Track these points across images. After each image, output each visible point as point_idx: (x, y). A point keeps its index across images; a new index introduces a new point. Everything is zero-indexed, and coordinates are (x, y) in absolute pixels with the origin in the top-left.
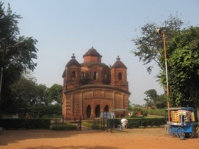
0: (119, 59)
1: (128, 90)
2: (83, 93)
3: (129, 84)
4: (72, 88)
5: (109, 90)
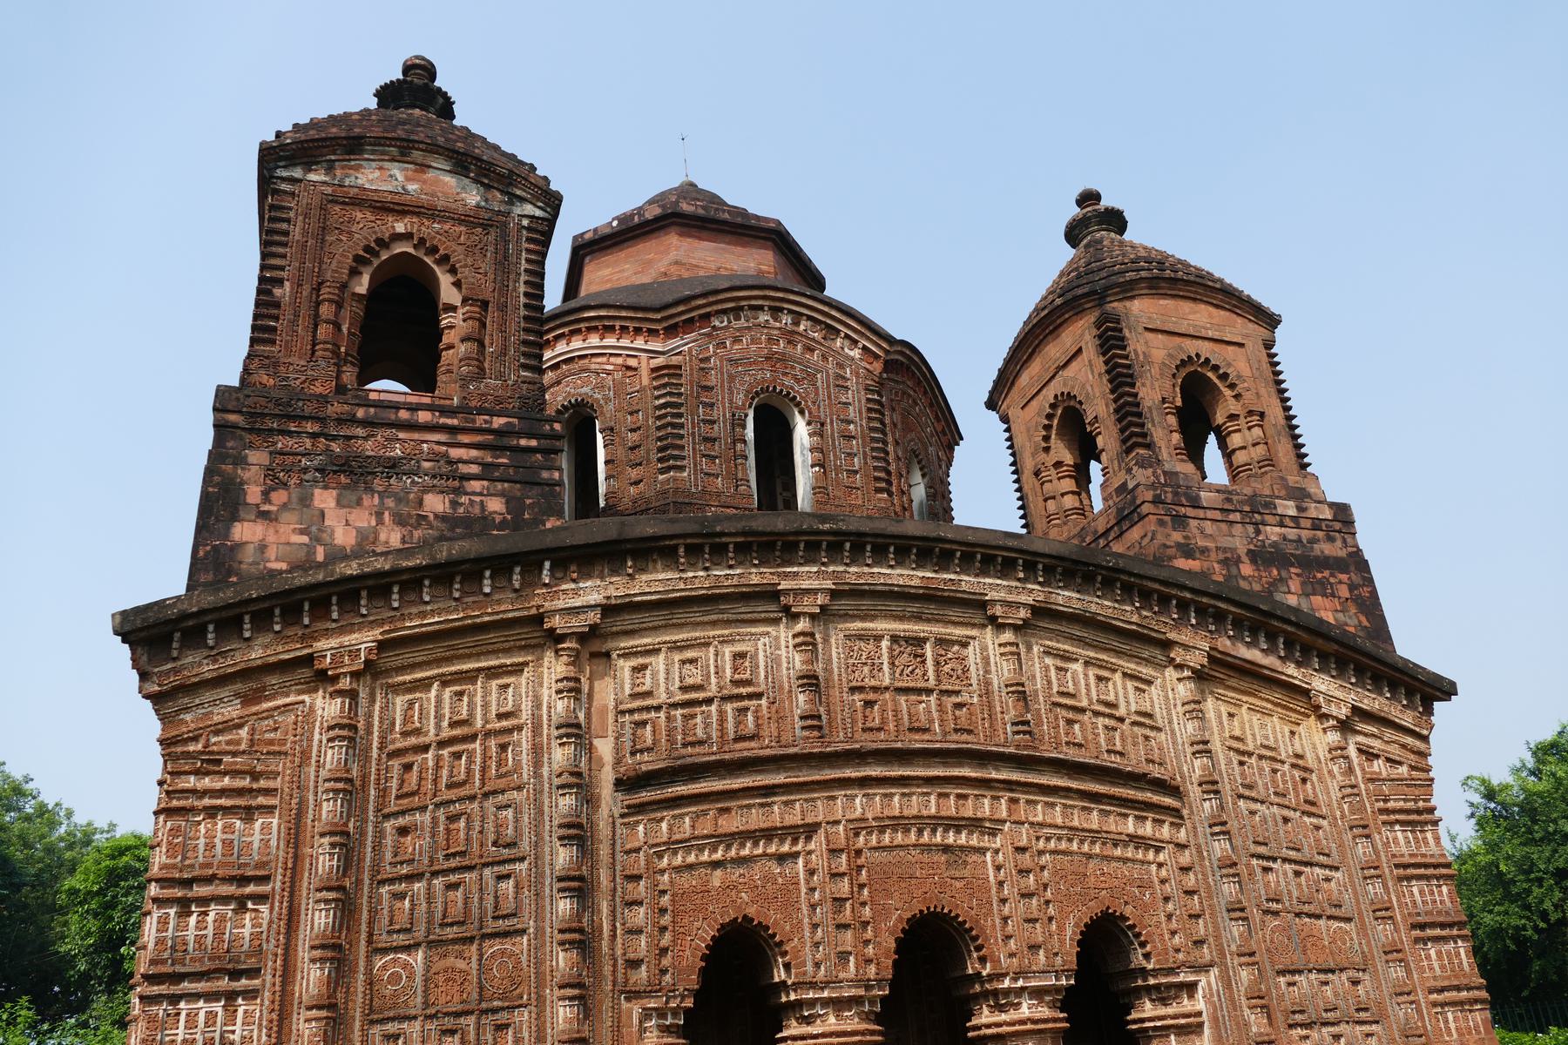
0: (1115, 220)
1: (1379, 629)
2: (593, 645)
3: (1367, 539)
4: (343, 537)
5: (1101, 605)
